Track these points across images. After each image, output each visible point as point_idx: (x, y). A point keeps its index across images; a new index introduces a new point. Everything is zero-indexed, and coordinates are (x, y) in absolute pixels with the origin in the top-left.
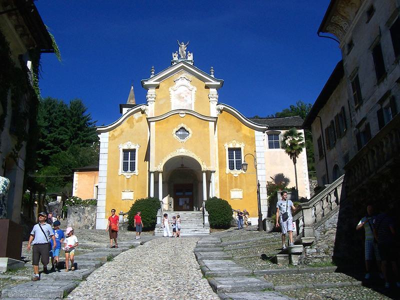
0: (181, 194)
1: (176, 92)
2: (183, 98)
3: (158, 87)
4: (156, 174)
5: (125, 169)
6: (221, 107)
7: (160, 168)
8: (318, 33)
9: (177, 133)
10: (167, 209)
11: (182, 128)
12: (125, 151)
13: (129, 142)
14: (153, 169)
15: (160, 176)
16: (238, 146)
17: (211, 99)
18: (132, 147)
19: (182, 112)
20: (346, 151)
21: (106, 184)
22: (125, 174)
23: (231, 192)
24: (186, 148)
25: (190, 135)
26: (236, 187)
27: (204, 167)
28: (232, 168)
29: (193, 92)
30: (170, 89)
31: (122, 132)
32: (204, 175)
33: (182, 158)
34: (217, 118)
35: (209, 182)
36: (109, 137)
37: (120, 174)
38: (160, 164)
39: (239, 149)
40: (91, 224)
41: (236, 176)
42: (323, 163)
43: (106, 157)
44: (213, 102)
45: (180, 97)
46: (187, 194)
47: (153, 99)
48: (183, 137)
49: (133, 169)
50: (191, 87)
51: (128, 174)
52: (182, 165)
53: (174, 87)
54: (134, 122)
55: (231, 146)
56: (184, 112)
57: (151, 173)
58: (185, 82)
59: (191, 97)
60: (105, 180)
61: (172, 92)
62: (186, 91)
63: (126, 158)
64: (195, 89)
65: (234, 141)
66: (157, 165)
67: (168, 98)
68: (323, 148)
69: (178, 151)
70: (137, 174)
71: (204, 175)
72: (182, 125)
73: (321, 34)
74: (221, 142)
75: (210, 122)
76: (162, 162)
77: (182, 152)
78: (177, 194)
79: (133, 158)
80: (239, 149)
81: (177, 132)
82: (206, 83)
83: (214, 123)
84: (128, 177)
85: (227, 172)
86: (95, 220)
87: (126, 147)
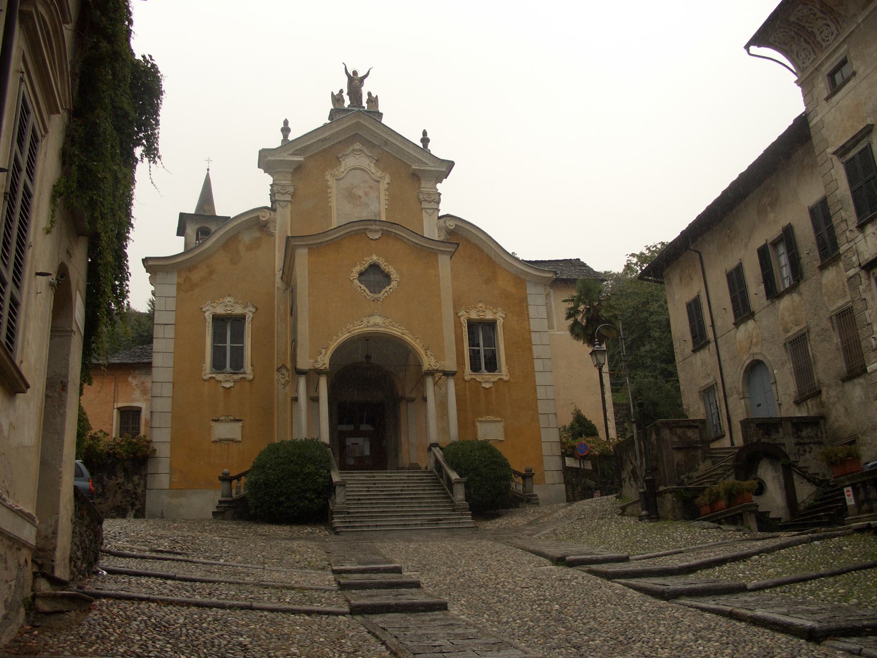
0: (350, 428)
2: (360, 197)
4: (312, 375)
5: (218, 365)
7: (324, 361)
8: (747, 47)
9: (363, 278)
11: (374, 267)
12: (219, 320)
13: (229, 299)
14: (304, 362)
16: (489, 316)
20: (797, 329)
21: (170, 400)
22: (220, 377)
23: (478, 424)
25: (394, 284)
26: (488, 413)
27: (428, 362)
28: (475, 368)
29: (383, 185)
30: (328, 177)
31: (211, 272)
33: (367, 339)
34: (458, 244)
36: (179, 285)
37: (206, 377)
38: (323, 351)
39: (492, 324)
40: (133, 505)
41: (487, 386)
42: (706, 355)
43: (170, 332)
44: (430, 211)
45: (351, 196)
46: (364, 427)
47: (288, 198)
48: (376, 288)
49: (238, 365)
50: (377, 173)
51: (226, 380)
52: (368, 357)
55: (474, 315)
56: (377, 228)
57: (300, 373)
58: (364, 162)
59: (379, 198)
60: (167, 390)
61: (331, 182)
62: (365, 182)
63: (218, 337)
64: (387, 180)
65: (481, 305)
67: (324, 195)
68: (708, 322)
69: (365, 320)
70: (250, 377)
72: (375, 258)
73: (754, 49)
74: (457, 306)
76: (327, 348)
78: (344, 428)
79: (238, 337)
80: (492, 324)
81: (361, 274)
84: (228, 385)
85: (467, 378)
86: (144, 491)
87: (220, 310)
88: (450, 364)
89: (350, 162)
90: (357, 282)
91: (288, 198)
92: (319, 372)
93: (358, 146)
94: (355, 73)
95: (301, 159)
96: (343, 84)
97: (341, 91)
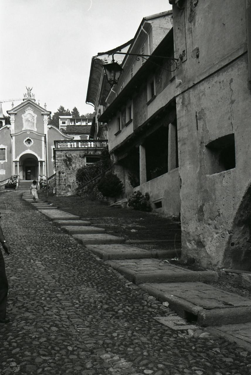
1: (26, 118)
3: (16, 114)
4: (16, 162)
6: (50, 126)
7: (18, 159)
8: (86, 102)
10: (22, 179)
14: (14, 159)
15: (18, 163)
17: (44, 122)
18: (4, 147)
19: (28, 131)
24: (31, 149)
27: (39, 159)
32: (39, 163)
35: (41, 165)
50: (33, 114)
53: (25, 114)
54: (4, 134)
66: (16, 158)
71: (39, 163)
75: (42, 137)
77: (29, 151)
81: (26, 141)
82: (42, 113)
83: (44, 137)
88: (43, 159)
89: (27, 112)
90: (25, 143)
91: (14, 121)
92: (17, 162)
93: (29, 108)
94: (29, 88)
95: (16, 112)
96: (26, 92)
97: (26, 94)
